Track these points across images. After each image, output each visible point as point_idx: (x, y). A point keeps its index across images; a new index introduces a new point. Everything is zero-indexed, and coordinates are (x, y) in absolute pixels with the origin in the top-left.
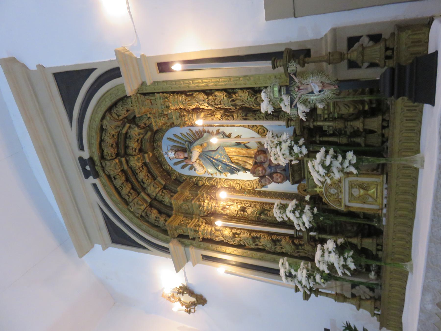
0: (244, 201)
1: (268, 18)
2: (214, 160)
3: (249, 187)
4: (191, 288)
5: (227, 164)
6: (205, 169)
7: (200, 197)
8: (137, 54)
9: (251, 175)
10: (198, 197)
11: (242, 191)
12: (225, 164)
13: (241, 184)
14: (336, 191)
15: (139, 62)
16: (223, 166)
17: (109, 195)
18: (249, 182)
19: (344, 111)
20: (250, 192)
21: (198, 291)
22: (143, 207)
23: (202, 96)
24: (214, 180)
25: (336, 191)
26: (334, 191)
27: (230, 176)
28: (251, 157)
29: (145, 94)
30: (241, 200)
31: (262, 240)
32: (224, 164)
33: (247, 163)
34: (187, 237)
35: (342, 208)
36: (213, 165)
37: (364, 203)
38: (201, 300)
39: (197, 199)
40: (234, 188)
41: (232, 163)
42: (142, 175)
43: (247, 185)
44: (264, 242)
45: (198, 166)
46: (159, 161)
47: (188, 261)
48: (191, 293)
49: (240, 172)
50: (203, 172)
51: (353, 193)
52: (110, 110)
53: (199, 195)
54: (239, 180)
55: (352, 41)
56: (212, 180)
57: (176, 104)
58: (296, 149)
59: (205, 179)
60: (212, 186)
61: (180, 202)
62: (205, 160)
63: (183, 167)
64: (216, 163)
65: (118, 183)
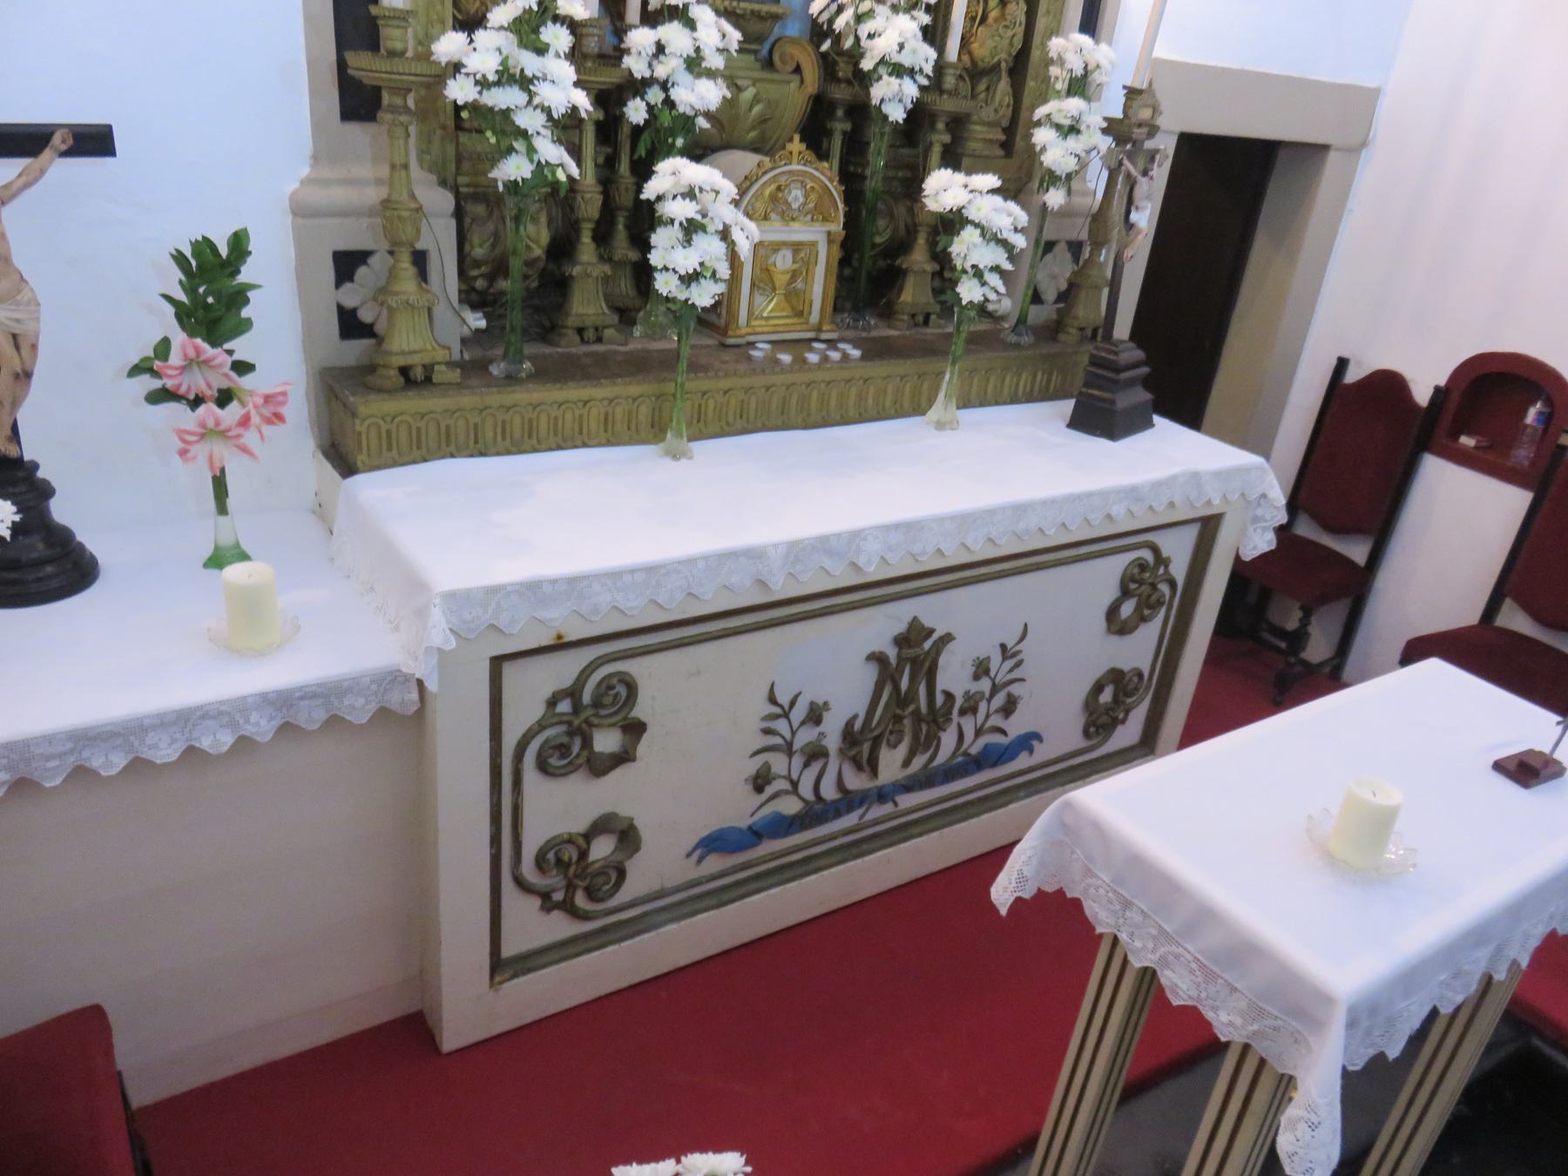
14: (795, 206)
25: (795, 206)
26: (796, 199)
37: (753, 285)
51: (781, 253)
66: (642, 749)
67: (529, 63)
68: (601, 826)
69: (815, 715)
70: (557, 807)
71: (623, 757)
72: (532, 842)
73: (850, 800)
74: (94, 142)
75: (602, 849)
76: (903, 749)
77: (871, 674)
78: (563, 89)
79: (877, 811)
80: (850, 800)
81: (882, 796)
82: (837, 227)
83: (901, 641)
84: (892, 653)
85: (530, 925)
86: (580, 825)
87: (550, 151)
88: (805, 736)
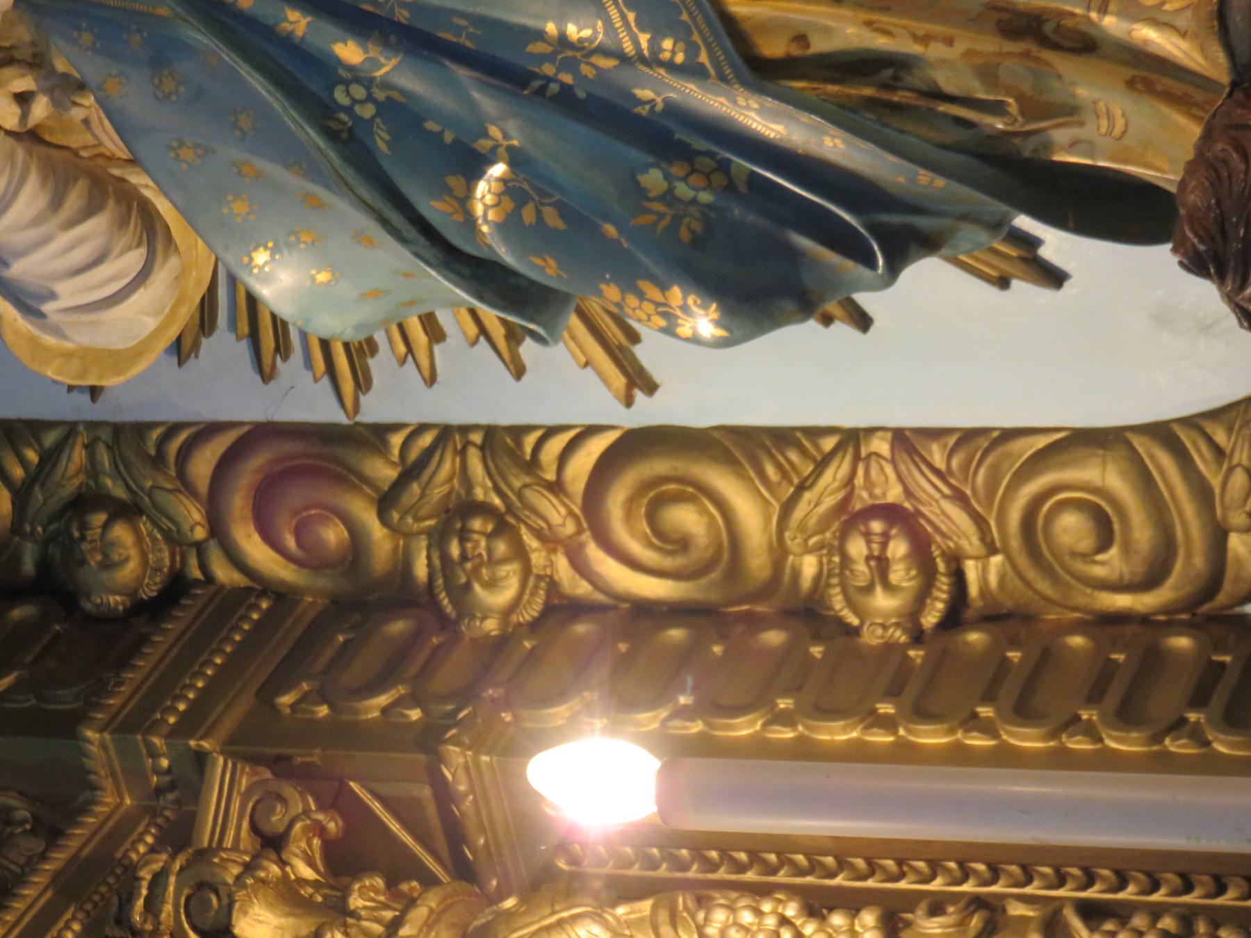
0: (1027, 862)
2: (350, 52)
3: (1111, 563)
5: (651, 92)
6: (193, 258)
7: (122, 830)
9: (1205, 295)
10: (79, 838)
11: (993, 659)
12: (601, 111)
13: (952, 522)
16: (566, 149)
18: (1108, 475)
20: (1152, 661)
24: (384, 472)
27: (712, 367)
30: (964, 857)
32: (566, 101)
33: (1086, 45)
36: (350, 142)
39: (70, 887)
40: (809, 614)
41: (762, 72)
43: (1071, 528)
45: (31, 199)
49: (927, 275)
50: (146, 316)
53: (113, 800)
54: (907, 441)
56: (350, 479)
59: (203, 465)
62: (161, 56)
64: (401, 113)
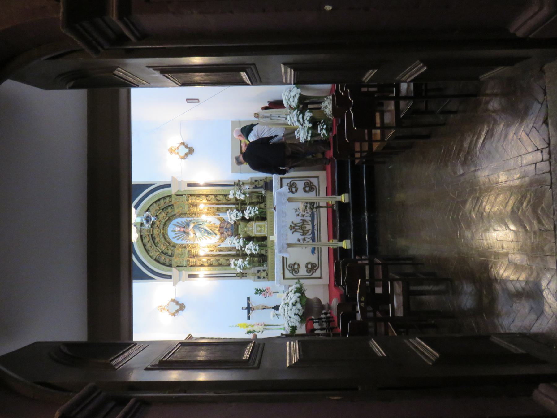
1: (233, 172)
4: (177, 300)
8: (179, 180)
15: (180, 183)
17: (139, 247)
19: (255, 200)
21: (180, 302)
22: (158, 253)
23: (204, 197)
28: (217, 227)
29: (177, 195)
31: (221, 260)
34: (182, 266)
35: (254, 235)
38: (182, 307)
42: (157, 240)
44: (222, 261)
46: (165, 236)
47: (180, 280)
48: (177, 303)
52: (155, 202)
55: (256, 181)
57: (191, 200)
58: (238, 214)
60: (193, 248)
61: (178, 252)
63: (178, 239)
65: (146, 241)
66: (298, 262)
67: (238, 265)
68: (306, 267)
69: (299, 240)
70: (303, 271)
71: (298, 265)
72: (307, 274)
73: (313, 233)
74: (249, 298)
75: (309, 266)
76: (307, 226)
77: (295, 233)
78: (240, 262)
79: (316, 228)
80: (313, 233)
81: (313, 227)
82: (254, 222)
83: (291, 230)
84: (293, 230)
85: (317, 274)
86: (306, 269)
87: (246, 263)
88: (301, 241)
